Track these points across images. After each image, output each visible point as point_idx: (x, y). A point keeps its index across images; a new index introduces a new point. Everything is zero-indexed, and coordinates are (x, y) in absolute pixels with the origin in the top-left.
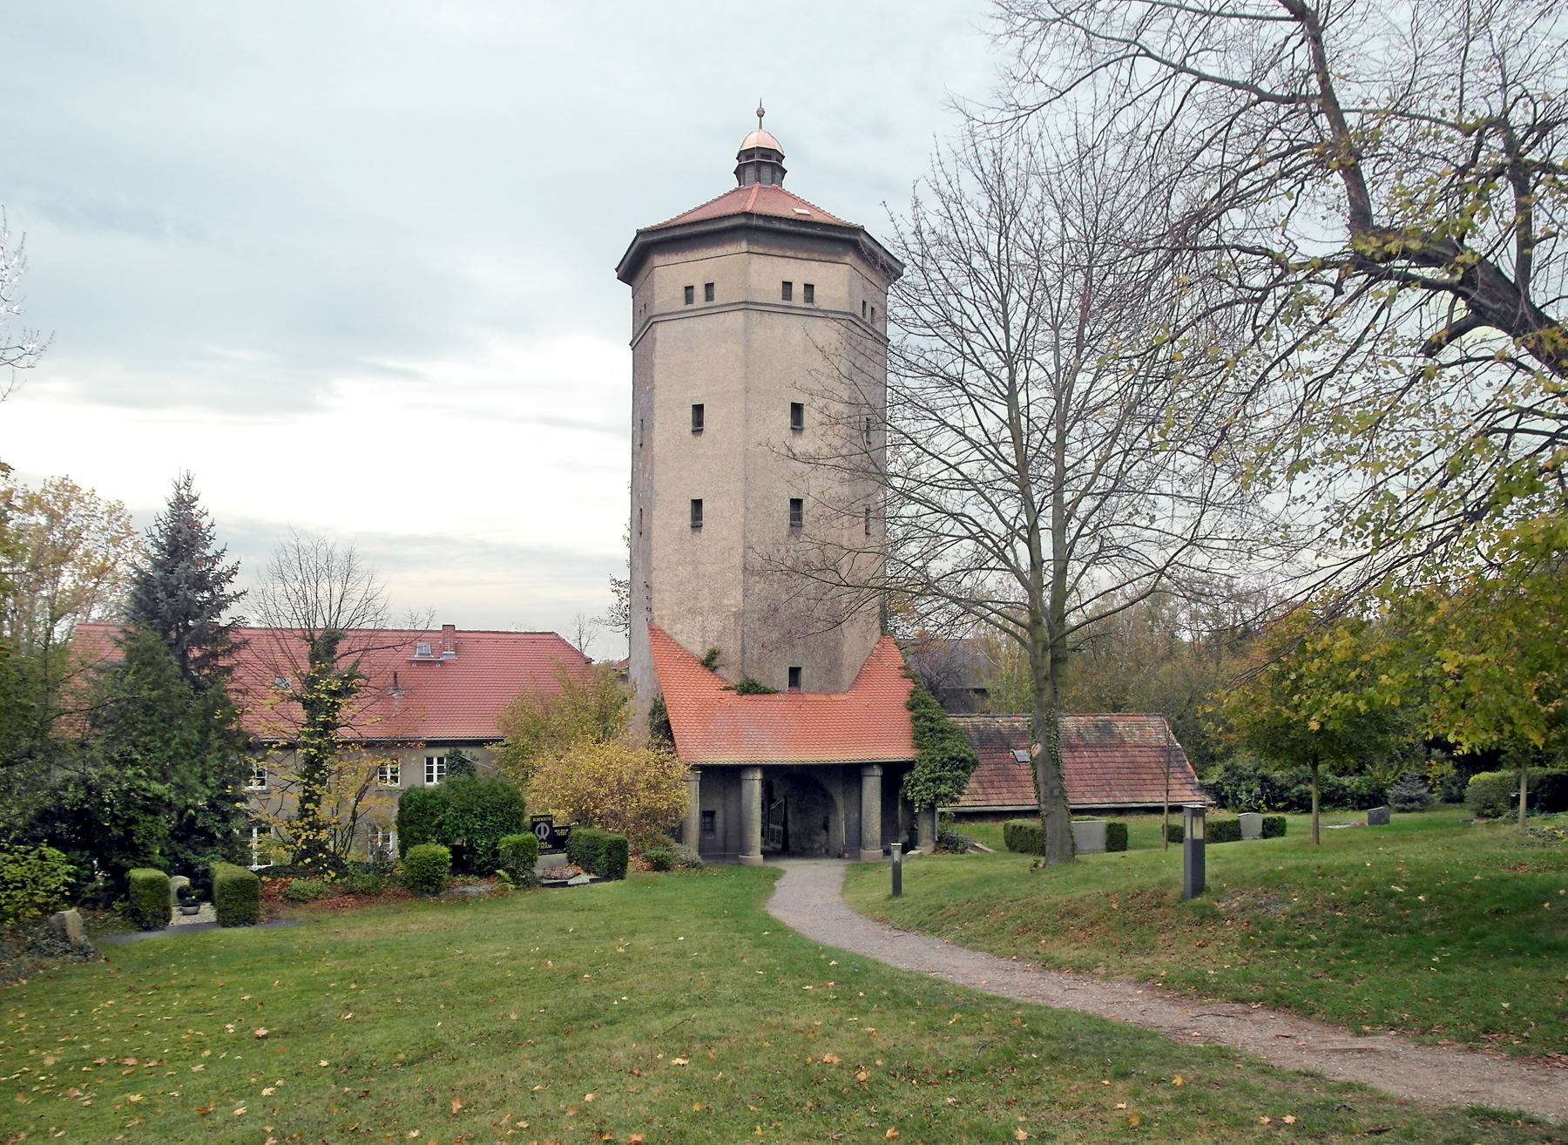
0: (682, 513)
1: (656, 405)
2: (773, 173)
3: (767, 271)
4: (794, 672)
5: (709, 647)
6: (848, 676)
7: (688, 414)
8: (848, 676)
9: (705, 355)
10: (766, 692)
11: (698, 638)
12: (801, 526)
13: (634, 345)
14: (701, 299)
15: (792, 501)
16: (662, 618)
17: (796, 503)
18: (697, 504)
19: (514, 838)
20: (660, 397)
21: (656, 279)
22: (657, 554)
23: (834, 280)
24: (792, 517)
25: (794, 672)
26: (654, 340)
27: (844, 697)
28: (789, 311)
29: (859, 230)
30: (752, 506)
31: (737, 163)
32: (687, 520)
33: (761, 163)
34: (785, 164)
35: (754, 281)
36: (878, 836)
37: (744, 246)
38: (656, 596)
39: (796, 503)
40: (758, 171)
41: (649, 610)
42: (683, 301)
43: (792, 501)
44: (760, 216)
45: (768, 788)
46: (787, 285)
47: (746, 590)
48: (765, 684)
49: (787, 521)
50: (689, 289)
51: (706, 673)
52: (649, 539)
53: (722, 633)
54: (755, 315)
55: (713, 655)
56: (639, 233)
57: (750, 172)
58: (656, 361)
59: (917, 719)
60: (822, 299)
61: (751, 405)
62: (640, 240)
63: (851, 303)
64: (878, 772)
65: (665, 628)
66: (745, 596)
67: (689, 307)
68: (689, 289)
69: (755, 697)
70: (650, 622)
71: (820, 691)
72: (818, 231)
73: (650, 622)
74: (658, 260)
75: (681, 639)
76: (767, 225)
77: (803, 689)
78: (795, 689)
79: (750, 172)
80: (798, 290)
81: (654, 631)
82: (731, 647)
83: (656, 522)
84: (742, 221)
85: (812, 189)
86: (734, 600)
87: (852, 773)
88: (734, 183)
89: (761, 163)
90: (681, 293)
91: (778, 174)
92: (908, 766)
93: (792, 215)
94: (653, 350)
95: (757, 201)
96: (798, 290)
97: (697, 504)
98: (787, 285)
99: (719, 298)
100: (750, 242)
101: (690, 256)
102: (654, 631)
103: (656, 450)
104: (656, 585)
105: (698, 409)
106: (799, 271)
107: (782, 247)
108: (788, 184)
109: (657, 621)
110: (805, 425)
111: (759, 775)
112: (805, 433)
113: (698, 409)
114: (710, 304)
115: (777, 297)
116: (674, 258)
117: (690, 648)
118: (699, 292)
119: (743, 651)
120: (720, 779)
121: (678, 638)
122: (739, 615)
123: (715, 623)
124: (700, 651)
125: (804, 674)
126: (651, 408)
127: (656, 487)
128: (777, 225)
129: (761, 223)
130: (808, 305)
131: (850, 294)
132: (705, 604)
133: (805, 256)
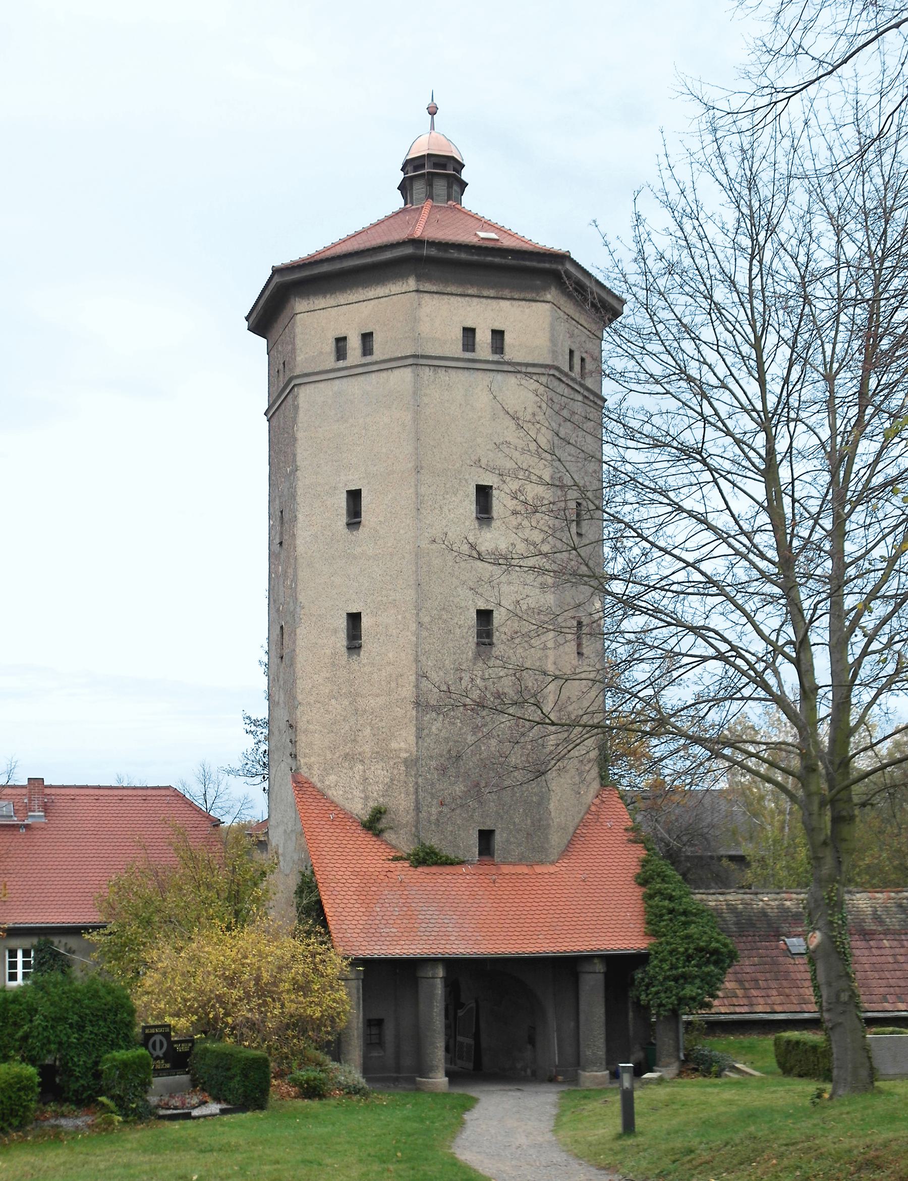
0: (335, 631)
1: (300, 492)
2: (450, 187)
3: (443, 315)
4: (486, 837)
5: (372, 804)
6: (556, 840)
7: (342, 501)
8: (556, 840)
9: (362, 426)
10: (449, 862)
11: (357, 793)
12: (491, 644)
13: (271, 414)
14: (358, 354)
15: (479, 612)
16: (310, 767)
17: (484, 616)
18: (354, 619)
19: (121, 1055)
20: (304, 480)
21: (298, 330)
22: (303, 685)
23: (530, 324)
24: (479, 635)
25: (486, 837)
26: (296, 408)
27: (552, 869)
28: (471, 365)
29: (564, 258)
30: (426, 620)
31: (401, 176)
32: (341, 639)
33: (434, 175)
34: (465, 175)
35: (425, 328)
36: (602, 1053)
37: (412, 283)
38: (302, 739)
39: (484, 616)
40: (430, 185)
41: (294, 756)
42: (333, 357)
43: (479, 612)
44: (432, 244)
45: (452, 988)
46: (469, 333)
47: (419, 729)
48: (448, 852)
49: (473, 639)
50: (341, 342)
51: (367, 839)
52: (292, 664)
53: (389, 787)
54: (427, 373)
55: (378, 814)
56: (276, 271)
57: (419, 188)
58: (300, 435)
59: (651, 897)
60: (514, 351)
61: (423, 490)
62: (277, 279)
63: (554, 352)
64: (600, 967)
65: (315, 780)
66: (419, 737)
67: (341, 364)
68: (341, 342)
69: (434, 869)
70: (296, 774)
71: (520, 861)
72: (509, 261)
73: (296, 774)
74: (300, 305)
75: (336, 794)
76: (441, 254)
77: (497, 859)
78: (485, 858)
79: (419, 188)
80: (483, 338)
81: (300, 784)
82: (401, 804)
83: (300, 643)
84: (409, 250)
85: (502, 203)
86: (404, 742)
87: (565, 968)
88: (397, 202)
89: (434, 175)
90: (330, 347)
91: (456, 188)
92: (639, 959)
93: (474, 240)
94: (294, 421)
95: (430, 225)
96: (483, 338)
97: (354, 619)
98: (469, 333)
99: (380, 351)
100: (419, 278)
101: (342, 298)
102: (300, 784)
103: (301, 548)
104: (301, 725)
105: (354, 496)
106: (485, 313)
107: (461, 283)
108: (469, 201)
109: (304, 771)
110: (495, 514)
111: (440, 972)
112: (496, 524)
113: (354, 496)
114: (369, 359)
115: (455, 349)
116: (320, 302)
117: (348, 806)
118: (354, 344)
119: (418, 809)
120: (386, 978)
121: (330, 793)
122: (411, 763)
123: (380, 773)
124: (359, 808)
125: (499, 839)
126: (293, 496)
127: (301, 598)
128: (455, 254)
129: (433, 252)
130: (496, 357)
131: (553, 340)
132: (367, 748)
133: (492, 293)
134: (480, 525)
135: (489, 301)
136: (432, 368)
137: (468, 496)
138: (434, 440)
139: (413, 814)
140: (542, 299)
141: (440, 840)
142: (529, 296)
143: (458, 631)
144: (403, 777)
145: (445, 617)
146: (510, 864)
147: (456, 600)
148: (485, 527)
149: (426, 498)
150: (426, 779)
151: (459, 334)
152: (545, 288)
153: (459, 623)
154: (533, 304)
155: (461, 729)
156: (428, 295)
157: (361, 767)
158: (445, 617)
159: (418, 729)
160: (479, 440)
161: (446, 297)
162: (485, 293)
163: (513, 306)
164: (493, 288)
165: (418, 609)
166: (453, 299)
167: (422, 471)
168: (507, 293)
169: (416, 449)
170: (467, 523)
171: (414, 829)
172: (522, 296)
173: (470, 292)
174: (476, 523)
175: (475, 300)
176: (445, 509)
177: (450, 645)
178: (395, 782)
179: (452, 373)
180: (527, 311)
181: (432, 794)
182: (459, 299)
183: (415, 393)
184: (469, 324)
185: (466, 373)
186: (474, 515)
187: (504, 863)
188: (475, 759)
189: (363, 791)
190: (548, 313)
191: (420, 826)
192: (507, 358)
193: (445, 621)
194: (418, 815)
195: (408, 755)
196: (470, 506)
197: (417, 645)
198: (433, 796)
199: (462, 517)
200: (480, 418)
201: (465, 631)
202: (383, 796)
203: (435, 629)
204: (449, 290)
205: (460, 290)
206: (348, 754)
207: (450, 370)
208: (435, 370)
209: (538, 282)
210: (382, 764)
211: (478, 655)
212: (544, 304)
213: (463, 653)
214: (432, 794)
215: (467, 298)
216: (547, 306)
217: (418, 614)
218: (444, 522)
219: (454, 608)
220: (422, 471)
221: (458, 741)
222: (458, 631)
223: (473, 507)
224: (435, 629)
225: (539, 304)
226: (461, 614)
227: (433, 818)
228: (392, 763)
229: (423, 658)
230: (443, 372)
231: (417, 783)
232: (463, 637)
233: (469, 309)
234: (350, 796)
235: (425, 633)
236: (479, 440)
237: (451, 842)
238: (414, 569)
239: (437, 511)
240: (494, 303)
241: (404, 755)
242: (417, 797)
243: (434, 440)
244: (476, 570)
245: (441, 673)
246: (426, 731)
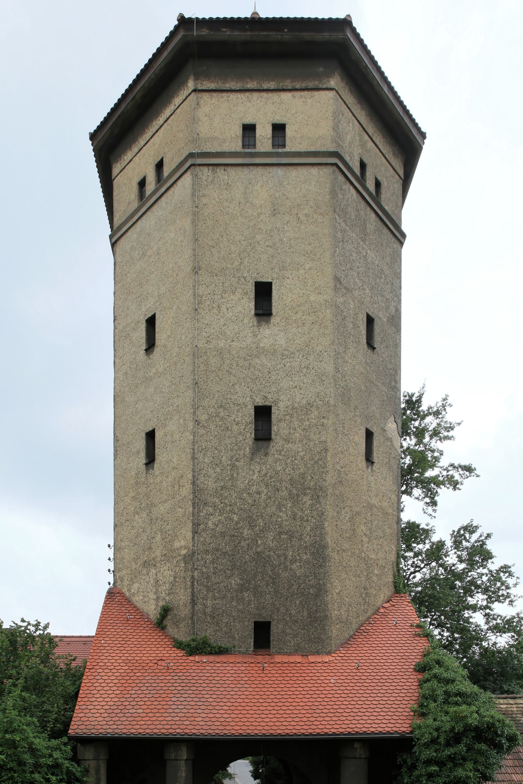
5: (161, 604)
6: (336, 632)
10: (221, 651)
17: (263, 413)
27: (327, 659)
30: (203, 418)
35: (204, 129)
39: (263, 413)
47: (196, 525)
48: (224, 643)
49: (250, 435)
55: (165, 612)
61: (201, 290)
75: (137, 600)
77: (272, 650)
80: (264, 133)
82: (182, 597)
96: (264, 133)
100: (197, 78)
112: (274, 320)
119: (193, 602)
122: (190, 558)
123: (166, 572)
133: (272, 85)
134: (259, 322)
135: (270, 94)
136: (211, 168)
137: (246, 294)
138: (212, 240)
139: (189, 607)
140: (325, 86)
141: (216, 631)
142: (311, 85)
143: (235, 427)
144: (182, 574)
145: (222, 414)
146: (286, 654)
147: (234, 397)
148: (264, 323)
149: (204, 298)
150: (202, 573)
151: (239, 132)
152: (329, 76)
153: (237, 420)
154: (316, 93)
155: (237, 523)
156: (207, 94)
157: (154, 571)
158: (222, 414)
159: (194, 524)
160: (258, 237)
161: (224, 95)
162: (265, 86)
163: (294, 97)
164: (273, 80)
165: (195, 408)
166: (233, 96)
167: (200, 272)
169: (194, 250)
170: (246, 321)
171: (190, 621)
172: (304, 85)
173: (250, 85)
174: (255, 320)
175: (255, 95)
176: (224, 308)
177: (228, 441)
178: (177, 580)
179: (232, 171)
180: (309, 101)
181: (207, 587)
182: (239, 95)
183: (193, 195)
184: (249, 121)
185: (246, 170)
186: (253, 312)
187: (279, 653)
188: (251, 553)
189: (156, 593)
190: (332, 102)
191: (195, 618)
192: (287, 149)
193: (222, 419)
194: (193, 607)
195: (187, 551)
196: (249, 305)
197: (194, 443)
198: (208, 589)
199: (241, 315)
200: (260, 214)
201: (243, 427)
202: (169, 594)
203: (213, 427)
204: (228, 86)
206: (146, 561)
207: (229, 169)
208: (213, 170)
209: (321, 69)
210: (168, 564)
211: (254, 452)
212: (327, 92)
213: (240, 449)
214: (207, 587)
215: (247, 94)
216: (331, 94)
217: (194, 413)
218: (222, 322)
219: (232, 405)
220: (200, 272)
221: (233, 536)
222: (235, 427)
223: (252, 305)
224: (213, 427)
225: (322, 93)
226: (238, 411)
227: (208, 610)
228: (175, 562)
229: (200, 456)
230: (222, 171)
231: (193, 576)
232: (240, 433)
233: (248, 104)
234: (147, 600)
235: (202, 431)
236: (258, 237)
237: (226, 633)
238: (192, 369)
239: (215, 311)
240: (275, 97)
241: (184, 552)
242: (193, 590)
243: (212, 240)
244: (254, 367)
245: (218, 470)
246: (202, 527)
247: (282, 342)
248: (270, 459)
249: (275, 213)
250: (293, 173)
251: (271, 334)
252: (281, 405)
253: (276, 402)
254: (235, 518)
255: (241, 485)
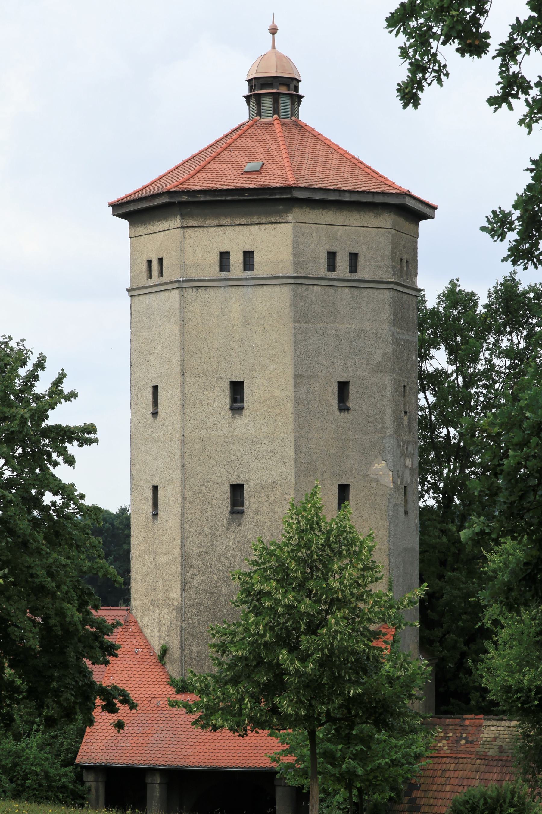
12: (242, 512)
17: (237, 490)
39: (237, 490)
46: (224, 256)
60: (261, 268)
80: (236, 259)
96: (236, 259)
98: (224, 256)
112: (246, 412)
133: (242, 221)
143: (215, 502)
168: (255, 219)
173: (225, 222)
205: (216, 222)
211: (230, 523)
222: (215, 502)
236: (232, 344)
247: (252, 430)
248: (243, 528)
249: (246, 323)
250: (261, 291)
251: (243, 424)
252: (252, 483)
253: (247, 481)
254: (215, 578)
255: (219, 550)
